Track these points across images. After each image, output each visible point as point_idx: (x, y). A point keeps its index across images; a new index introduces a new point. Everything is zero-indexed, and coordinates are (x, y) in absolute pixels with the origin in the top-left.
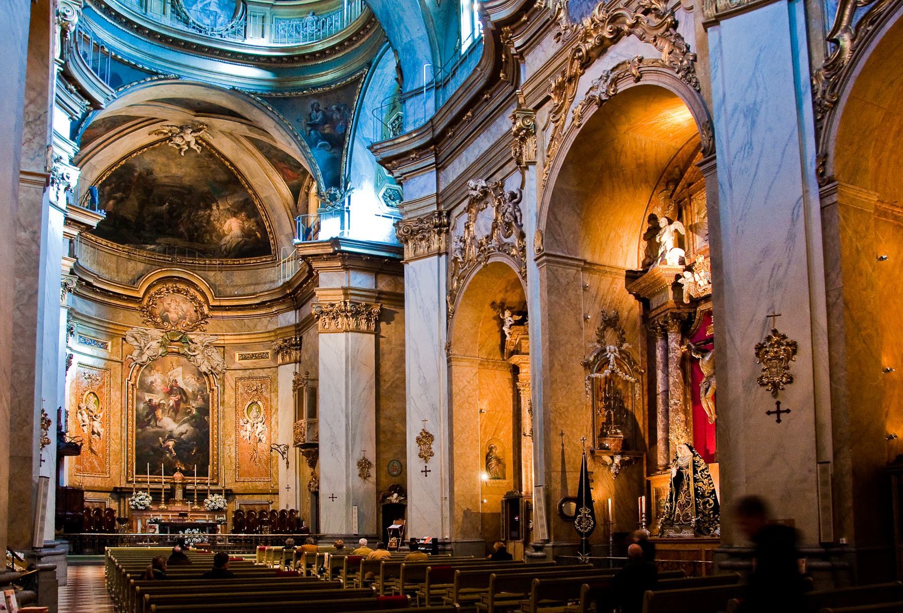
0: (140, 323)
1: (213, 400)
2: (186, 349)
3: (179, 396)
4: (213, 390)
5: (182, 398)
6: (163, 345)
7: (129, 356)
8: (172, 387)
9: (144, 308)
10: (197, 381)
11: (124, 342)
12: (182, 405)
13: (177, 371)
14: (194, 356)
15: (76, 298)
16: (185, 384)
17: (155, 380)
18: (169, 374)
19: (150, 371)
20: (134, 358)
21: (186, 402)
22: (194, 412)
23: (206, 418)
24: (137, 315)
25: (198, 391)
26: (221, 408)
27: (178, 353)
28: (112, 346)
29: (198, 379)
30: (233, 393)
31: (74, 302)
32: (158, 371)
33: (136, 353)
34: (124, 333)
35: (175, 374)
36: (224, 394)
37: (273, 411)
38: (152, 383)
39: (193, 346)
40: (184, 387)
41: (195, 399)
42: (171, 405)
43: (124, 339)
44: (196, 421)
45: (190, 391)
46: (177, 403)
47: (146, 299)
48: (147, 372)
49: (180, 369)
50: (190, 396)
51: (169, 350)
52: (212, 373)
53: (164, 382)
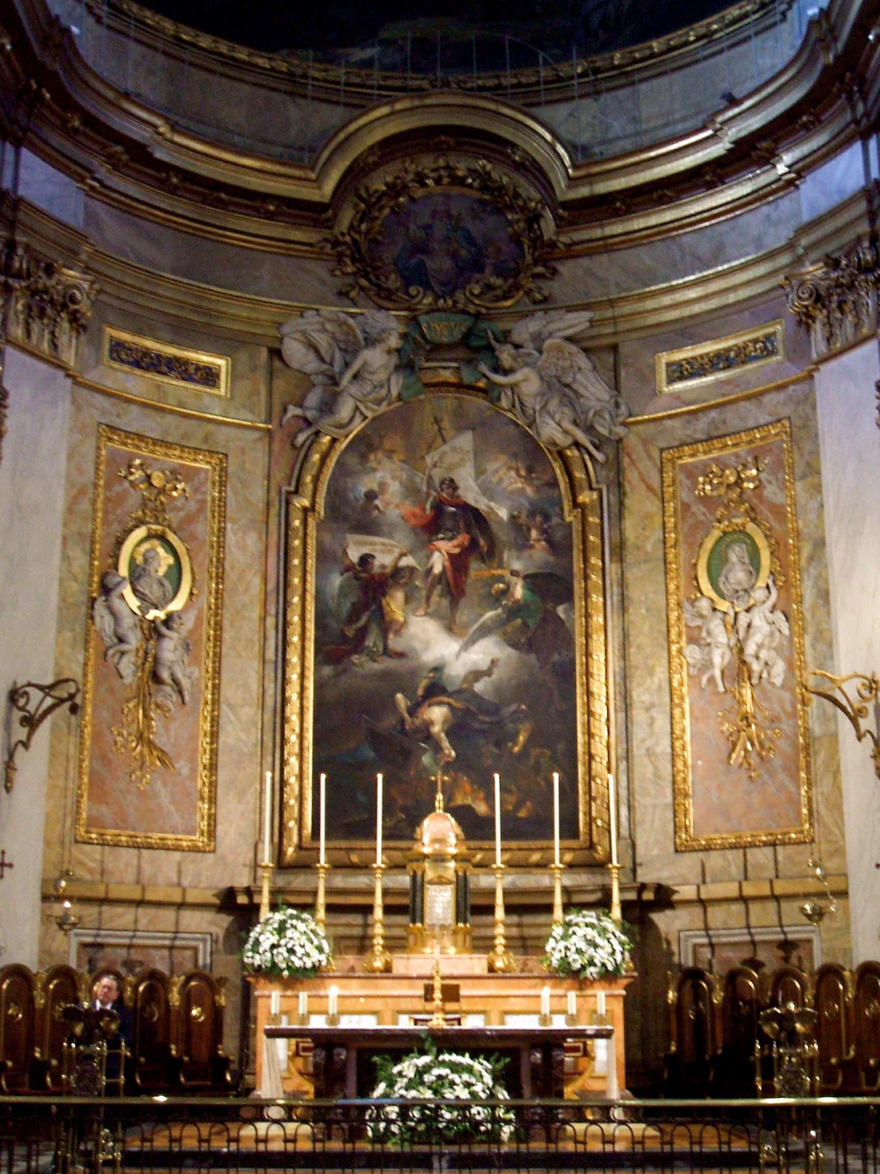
0: (330, 296)
1: (585, 541)
2: (484, 368)
3: (463, 538)
4: (583, 507)
5: (474, 543)
6: (406, 365)
7: (293, 411)
8: (439, 507)
9: (336, 243)
10: (528, 479)
11: (277, 364)
12: (476, 569)
13: (454, 449)
14: (513, 387)
15: (98, 207)
16: (487, 491)
17: (383, 485)
18: (429, 460)
19: (364, 458)
20: (310, 415)
21: (491, 555)
22: (519, 591)
23: (561, 610)
24: (320, 269)
25: (532, 514)
26: (612, 569)
27: (459, 386)
28: (235, 376)
29: (530, 470)
30: (653, 507)
31: (91, 217)
32: (390, 453)
33: (313, 399)
34: (273, 332)
35: (451, 459)
36: (621, 516)
37: (806, 550)
38: (371, 496)
39: (506, 355)
40: (481, 504)
41: (523, 544)
42: (437, 569)
43: (276, 353)
44: (525, 624)
45: (503, 513)
46: (458, 563)
47: (347, 217)
48: (353, 461)
49: (466, 440)
50: (503, 535)
51: (429, 377)
52: (577, 445)
53: (411, 491)
